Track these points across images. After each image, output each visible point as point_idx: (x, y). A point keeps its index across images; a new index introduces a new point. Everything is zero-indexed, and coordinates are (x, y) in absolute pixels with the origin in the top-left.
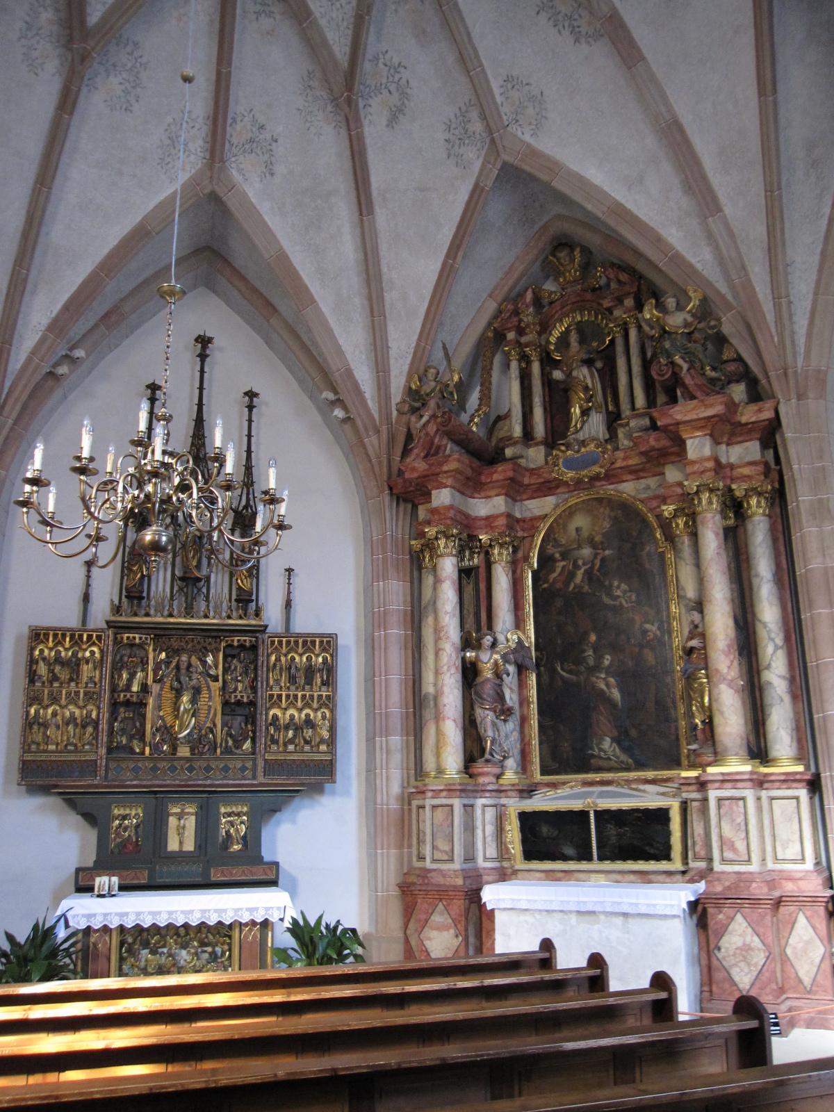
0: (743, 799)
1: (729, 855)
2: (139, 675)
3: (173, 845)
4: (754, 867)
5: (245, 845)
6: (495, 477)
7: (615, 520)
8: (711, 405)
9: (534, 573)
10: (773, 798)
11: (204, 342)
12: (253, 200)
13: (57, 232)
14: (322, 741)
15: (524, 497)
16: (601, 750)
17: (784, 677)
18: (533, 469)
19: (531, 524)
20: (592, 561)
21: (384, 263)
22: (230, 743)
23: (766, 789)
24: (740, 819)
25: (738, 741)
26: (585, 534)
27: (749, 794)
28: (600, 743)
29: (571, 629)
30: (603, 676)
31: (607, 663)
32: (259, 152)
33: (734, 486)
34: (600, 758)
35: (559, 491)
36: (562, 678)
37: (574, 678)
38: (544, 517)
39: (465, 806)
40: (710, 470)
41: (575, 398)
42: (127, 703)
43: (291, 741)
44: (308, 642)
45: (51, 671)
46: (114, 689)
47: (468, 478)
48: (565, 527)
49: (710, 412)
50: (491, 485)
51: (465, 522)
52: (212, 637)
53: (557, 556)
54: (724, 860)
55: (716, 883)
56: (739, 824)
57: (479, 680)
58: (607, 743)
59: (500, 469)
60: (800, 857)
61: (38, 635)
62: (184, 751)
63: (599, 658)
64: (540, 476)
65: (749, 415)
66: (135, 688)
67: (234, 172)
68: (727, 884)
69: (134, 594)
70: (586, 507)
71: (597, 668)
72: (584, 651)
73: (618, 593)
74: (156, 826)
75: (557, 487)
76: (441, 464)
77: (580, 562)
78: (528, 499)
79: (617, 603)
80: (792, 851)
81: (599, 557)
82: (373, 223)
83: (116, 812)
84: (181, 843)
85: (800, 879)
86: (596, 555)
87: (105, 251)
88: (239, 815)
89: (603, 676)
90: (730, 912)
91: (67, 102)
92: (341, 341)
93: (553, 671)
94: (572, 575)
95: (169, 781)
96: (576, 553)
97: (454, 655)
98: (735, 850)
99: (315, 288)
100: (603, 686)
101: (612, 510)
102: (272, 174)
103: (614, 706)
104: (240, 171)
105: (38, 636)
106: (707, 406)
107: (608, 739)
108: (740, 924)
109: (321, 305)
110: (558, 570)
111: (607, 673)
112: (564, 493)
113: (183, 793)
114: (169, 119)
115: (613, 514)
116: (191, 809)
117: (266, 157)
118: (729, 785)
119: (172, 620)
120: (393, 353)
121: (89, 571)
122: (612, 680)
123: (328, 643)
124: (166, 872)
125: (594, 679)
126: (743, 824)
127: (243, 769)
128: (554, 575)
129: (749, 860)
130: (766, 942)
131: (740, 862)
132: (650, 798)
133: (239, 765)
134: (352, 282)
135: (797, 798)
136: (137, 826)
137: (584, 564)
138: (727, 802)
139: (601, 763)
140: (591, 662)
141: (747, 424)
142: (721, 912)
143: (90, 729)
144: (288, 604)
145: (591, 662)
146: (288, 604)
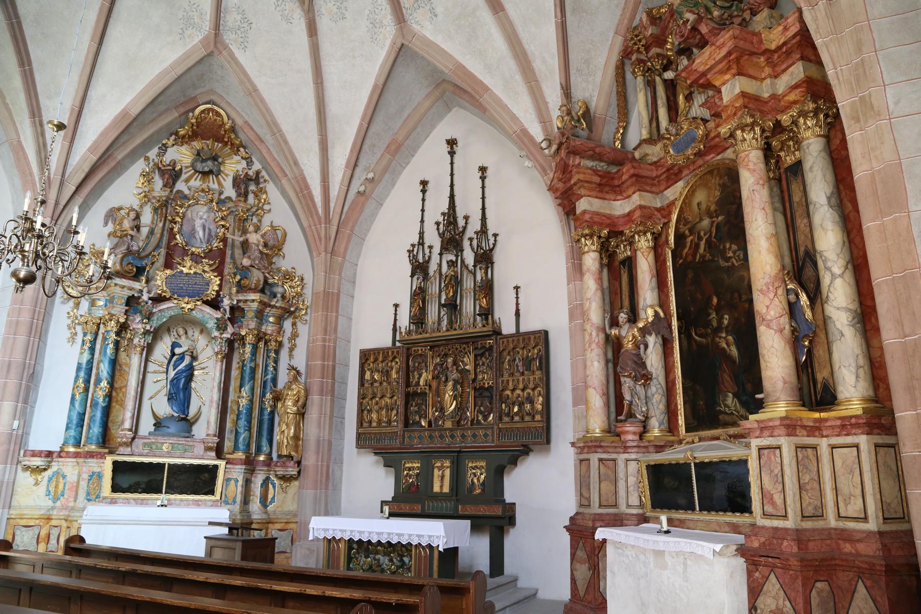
0: (779, 448)
1: (769, 509)
2: (424, 375)
3: (436, 489)
4: (789, 524)
5: (483, 490)
6: (625, 177)
7: (723, 187)
8: (723, 44)
9: (672, 252)
10: (833, 447)
11: (452, 143)
12: (432, 38)
13: (333, 108)
14: (537, 412)
15: (662, 188)
16: (726, 406)
17: (848, 310)
18: (655, 163)
19: (665, 211)
20: (710, 231)
21: (524, 42)
22: (480, 417)
23: (827, 436)
24: (777, 471)
25: (780, 385)
26: (704, 207)
27: (786, 443)
28: (725, 400)
29: (699, 296)
30: (724, 335)
31: (726, 322)
32: (423, 5)
33: (779, 118)
34: (727, 414)
35: (683, 174)
36: (696, 340)
37: (703, 340)
38: (672, 203)
39: (601, 460)
40: (740, 108)
41: (678, 88)
42: (415, 394)
43: (517, 414)
44: (523, 338)
45: (372, 377)
46: (408, 384)
47: (600, 185)
48: (690, 204)
49: (724, 52)
50: (625, 185)
51: (608, 222)
52: (465, 343)
53: (687, 232)
54: (765, 515)
55: (753, 538)
56: (777, 475)
57: (622, 350)
58: (730, 400)
59: (624, 170)
60: (862, 516)
61: (365, 355)
62: (449, 424)
63: (720, 321)
64: (662, 166)
65: (775, 38)
66: (421, 383)
67: (414, 25)
68: (763, 540)
69: (418, 319)
70: (702, 182)
71: (719, 329)
72: (709, 315)
73: (731, 254)
74: (426, 475)
75: (680, 171)
76: (570, 180)
77: (702, 234)
78: (666, 189)
79: (730, 264)
80: (854, 508)
81: (715, 225)
82: (507, 17)
83: (407, 465)
84: (441, 487)
85: (859, 541)
86: (713, 222)
87: (363, 107)
88: (481, 468)
89: (724, 335)
90: (765, 571)
91: (312, 30)
92: (515, 111)
93: (690, 337)
94: (697, 246)
95: (437, 444)
96: (699, 226)
97: (594, 334)
98: (773, 503)
99: (487, 80)
100: (725, 346)
101: (721, 178)
102: (436, 16)
103: (735, 362)
104: (417, 22)
105: (365, 355)
106: (720, 48)
107: (730, 395)
108: (774, 585)
109: (495, 91)
110: (688, 245)
111: (727, 332)
112: (687, 175)
113: (442, 453)
114: (367, 12)
115: (721, 182)
116: (447, 464)
117: (429, 5)
118: (766, 433)
119: (434, 335)
120: (551, 106)
121: (396, 311)
122: (730, 338)
123: (543, 337)
124: (430, 506)
125: (717, 339)
126: (780, 475)
127: (486, 435)
128: (686, 250)
129: (785, 516)
130: (796, 608)
131: (777, 517)
132: (733, 452)
133: (481, 432)
134: (511, 66)
135: (857, 446)
136: (418, 475)
137: (705, 235)
138: (766, 452)
139: (727, 418)
140: (715, 324)
141: (779, 48)
142: (757, 570)
143: (394, 412)
144: (517, 314)
145: (715, 324)
146: (517, 314)
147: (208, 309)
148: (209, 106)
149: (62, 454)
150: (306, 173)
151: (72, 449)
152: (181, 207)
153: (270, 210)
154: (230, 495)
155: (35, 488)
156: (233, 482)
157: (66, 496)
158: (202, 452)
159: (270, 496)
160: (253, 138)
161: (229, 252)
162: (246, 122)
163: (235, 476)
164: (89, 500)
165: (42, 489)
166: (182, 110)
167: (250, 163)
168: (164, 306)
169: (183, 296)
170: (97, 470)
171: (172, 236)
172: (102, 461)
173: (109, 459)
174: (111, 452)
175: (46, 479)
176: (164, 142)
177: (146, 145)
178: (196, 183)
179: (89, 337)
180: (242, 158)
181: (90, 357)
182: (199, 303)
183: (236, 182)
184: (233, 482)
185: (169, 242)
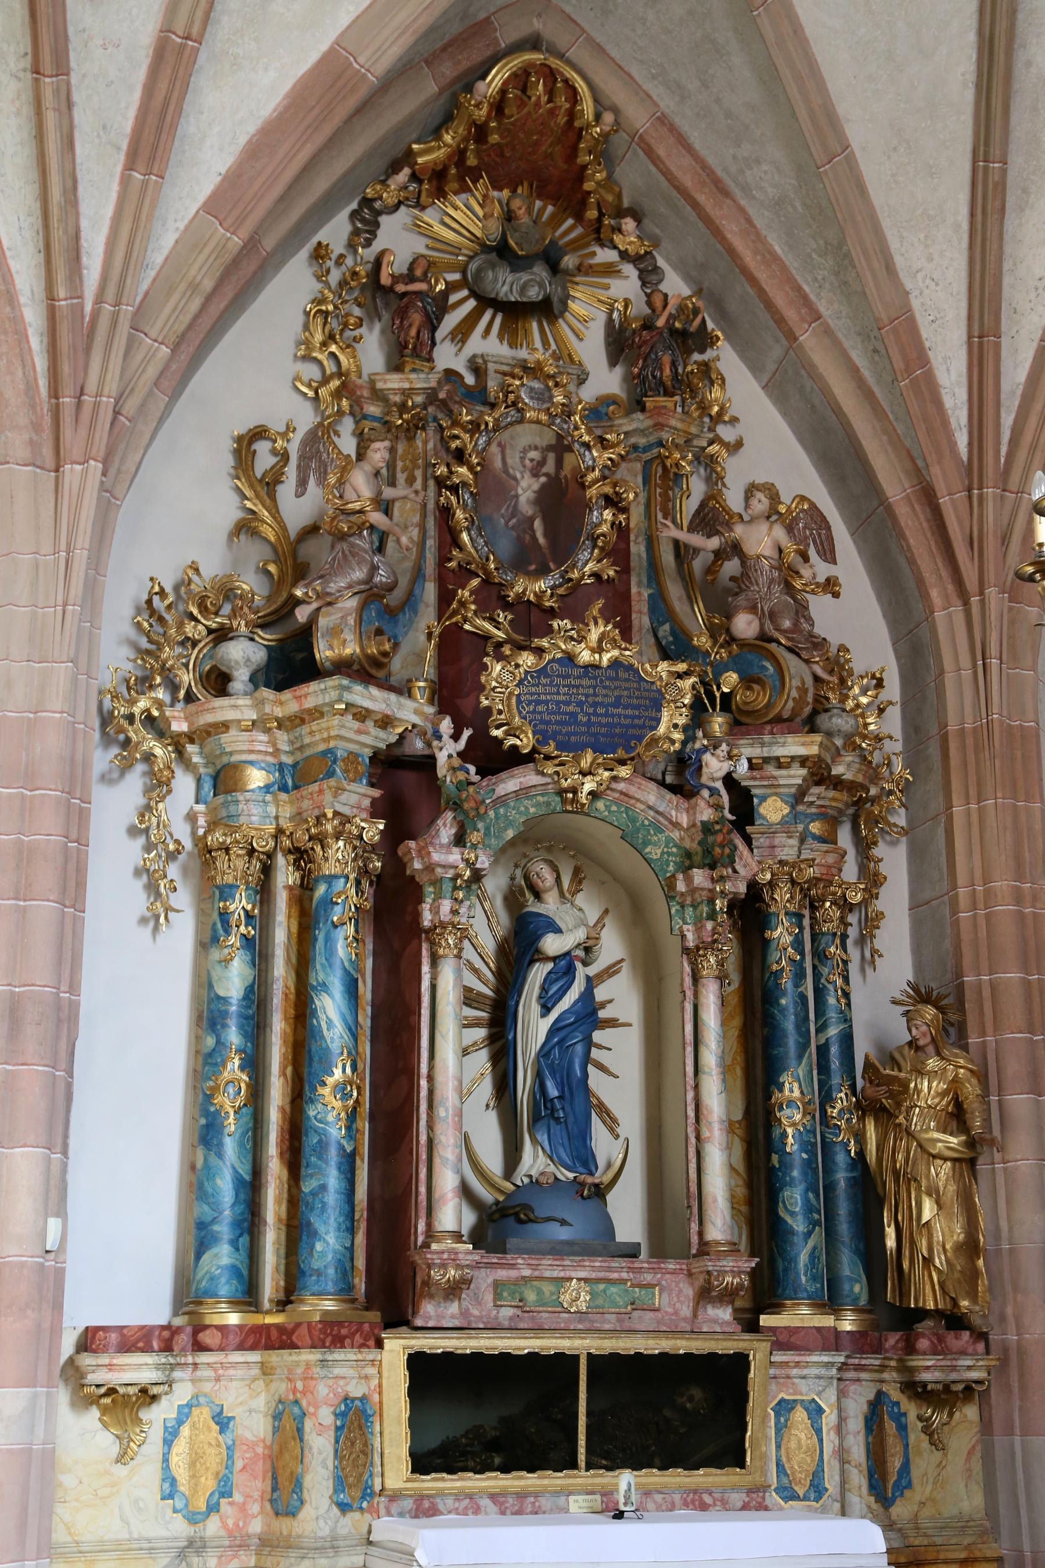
147: (651, 795)
148: (536, 57)
149: (206, 1337)
150: (915, 303)
151: (233, 1319)
152: (475, 427)
153: (739, 444)
154: (800, 1464)
155: (121, 1471)
156: (800, 1415)
157: (237, 1497)
159: (895, 1464)
160: (688, 181)
161: (640, 593)
162: (663, 120)
163: (806, 1390)
164: (344, 1508)
165: (146, 1471)
166: (449, 70)
167: (649, 275)
168: (510, 783)
169: (577, 749)
170: (356, 1390)
171: (449, 536)
172: (372, 1354)
173: (397, 1348)
174: (398, 1318)
175: (155, 1435)
176: (369, 192)
177: (322, 211)
178: (488, 343)
179: (240, 903)
180: (624, 255)
181: (249, 974)
182: (624, 772)
183: (620, 343)
184: (800, 1415)
185: (443, 559)
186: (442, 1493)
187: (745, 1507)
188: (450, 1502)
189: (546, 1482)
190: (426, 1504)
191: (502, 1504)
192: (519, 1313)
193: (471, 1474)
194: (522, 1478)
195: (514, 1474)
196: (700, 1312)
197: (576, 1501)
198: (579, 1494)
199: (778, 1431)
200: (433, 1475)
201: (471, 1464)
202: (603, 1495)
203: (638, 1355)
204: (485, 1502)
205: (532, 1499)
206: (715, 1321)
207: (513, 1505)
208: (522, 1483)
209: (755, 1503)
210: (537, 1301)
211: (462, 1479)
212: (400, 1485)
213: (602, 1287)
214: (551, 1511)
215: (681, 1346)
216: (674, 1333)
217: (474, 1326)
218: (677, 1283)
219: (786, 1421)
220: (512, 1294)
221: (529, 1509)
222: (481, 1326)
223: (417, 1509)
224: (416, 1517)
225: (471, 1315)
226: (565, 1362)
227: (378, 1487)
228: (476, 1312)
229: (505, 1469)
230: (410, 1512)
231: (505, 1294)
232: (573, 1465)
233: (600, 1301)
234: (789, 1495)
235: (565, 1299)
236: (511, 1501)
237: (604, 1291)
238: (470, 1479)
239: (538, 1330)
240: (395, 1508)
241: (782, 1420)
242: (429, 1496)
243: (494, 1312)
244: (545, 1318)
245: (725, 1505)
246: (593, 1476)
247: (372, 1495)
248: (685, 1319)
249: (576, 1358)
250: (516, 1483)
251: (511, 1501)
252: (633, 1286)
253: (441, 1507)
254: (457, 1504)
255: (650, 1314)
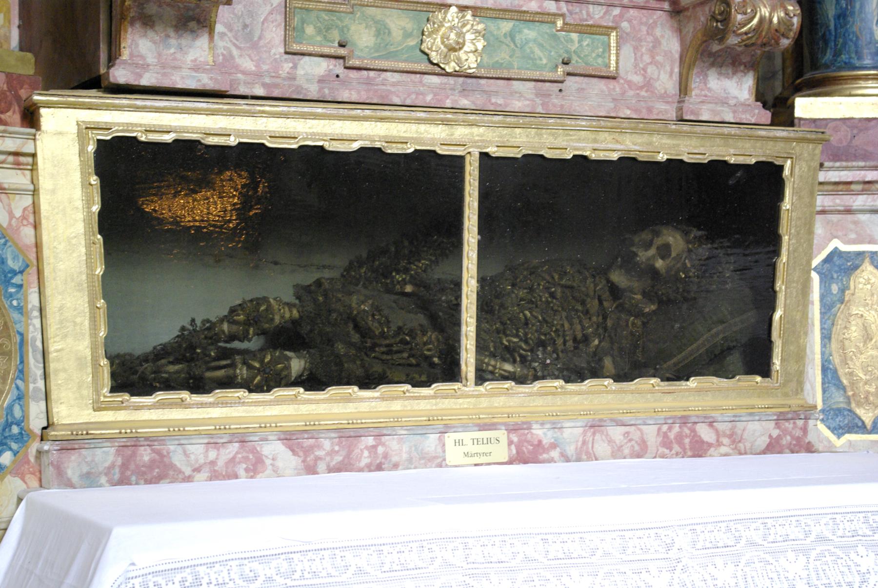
158: (666, 81)
186: (179, 433)
187: (773, 447)
188: (197, 451)
189: (397, 406)
190: (145, 455)
191: (308, 451)
192: (340, 70)
193: (242, 393)
194: (349, 399)
195: (333, 391)
196: (695, 83)
197: (459, 443)
198: (465, 428)
199: (827, 308)
200: (160, 396)
201: (242, 372)
202: (512, 429)
203: (581, 160)
204: (274, 449)
205: (370, 441)
206: (724, 102)
207: (332, 453)
208: (351, 408)
209: (790, 439)
210: (377, 48)
211: (225, 404)
212: (87, 416)
213: (506, 26)
214: (410, 464)
215: (661, 148)
216: (641, 123)
217: (242, 91)
218: (651, 28)
219: (842, 291)
220: (324, 30)
221: (365, 461)
222: (260, 91)
223: (124, 466)
224: (123, 481)
225: (237, 68)
226: (433, 173)
227: (36, 422)
228: (248, 64)
229: (313, 382)
230: (108, 471)
231: (310, 30)
232: (450, 371)
233: (503, 55)
234: (846, 422)
235: (435, 45)
236: (327, 444)
237: (511, 35)
238: (240, 402)
239: (378, 106)
240: (73, 466)
241: (835, 288)
242: (150, 440)
243: (287, 66)
244: (395, 86)
245: (738, 446)
246: (490, 395)
247: (23, 437)
248: (664, 97)
249: (456, 163)
250: (338, 409)
251: (327, 444)
252: (568, 27)
253: (178, 460)
254: (212, 454)
255: (601, 84)
